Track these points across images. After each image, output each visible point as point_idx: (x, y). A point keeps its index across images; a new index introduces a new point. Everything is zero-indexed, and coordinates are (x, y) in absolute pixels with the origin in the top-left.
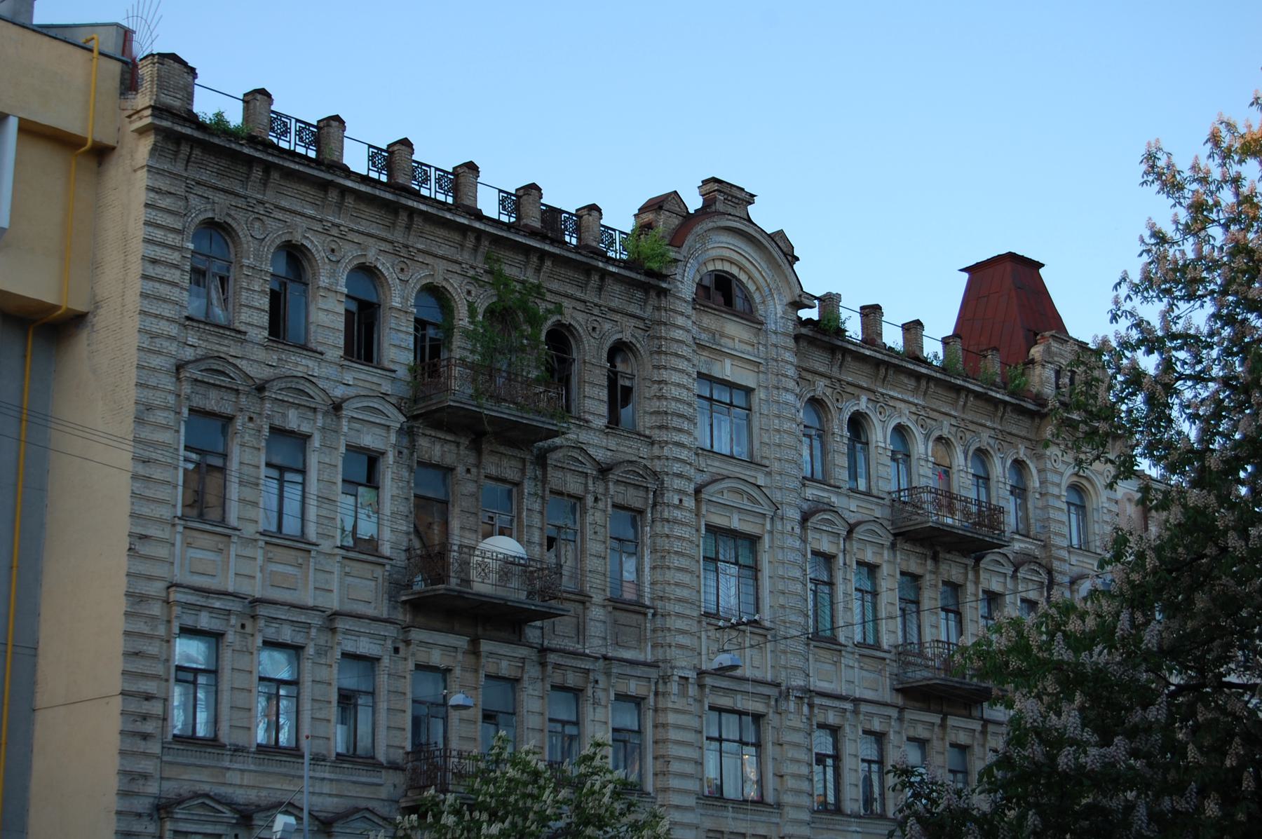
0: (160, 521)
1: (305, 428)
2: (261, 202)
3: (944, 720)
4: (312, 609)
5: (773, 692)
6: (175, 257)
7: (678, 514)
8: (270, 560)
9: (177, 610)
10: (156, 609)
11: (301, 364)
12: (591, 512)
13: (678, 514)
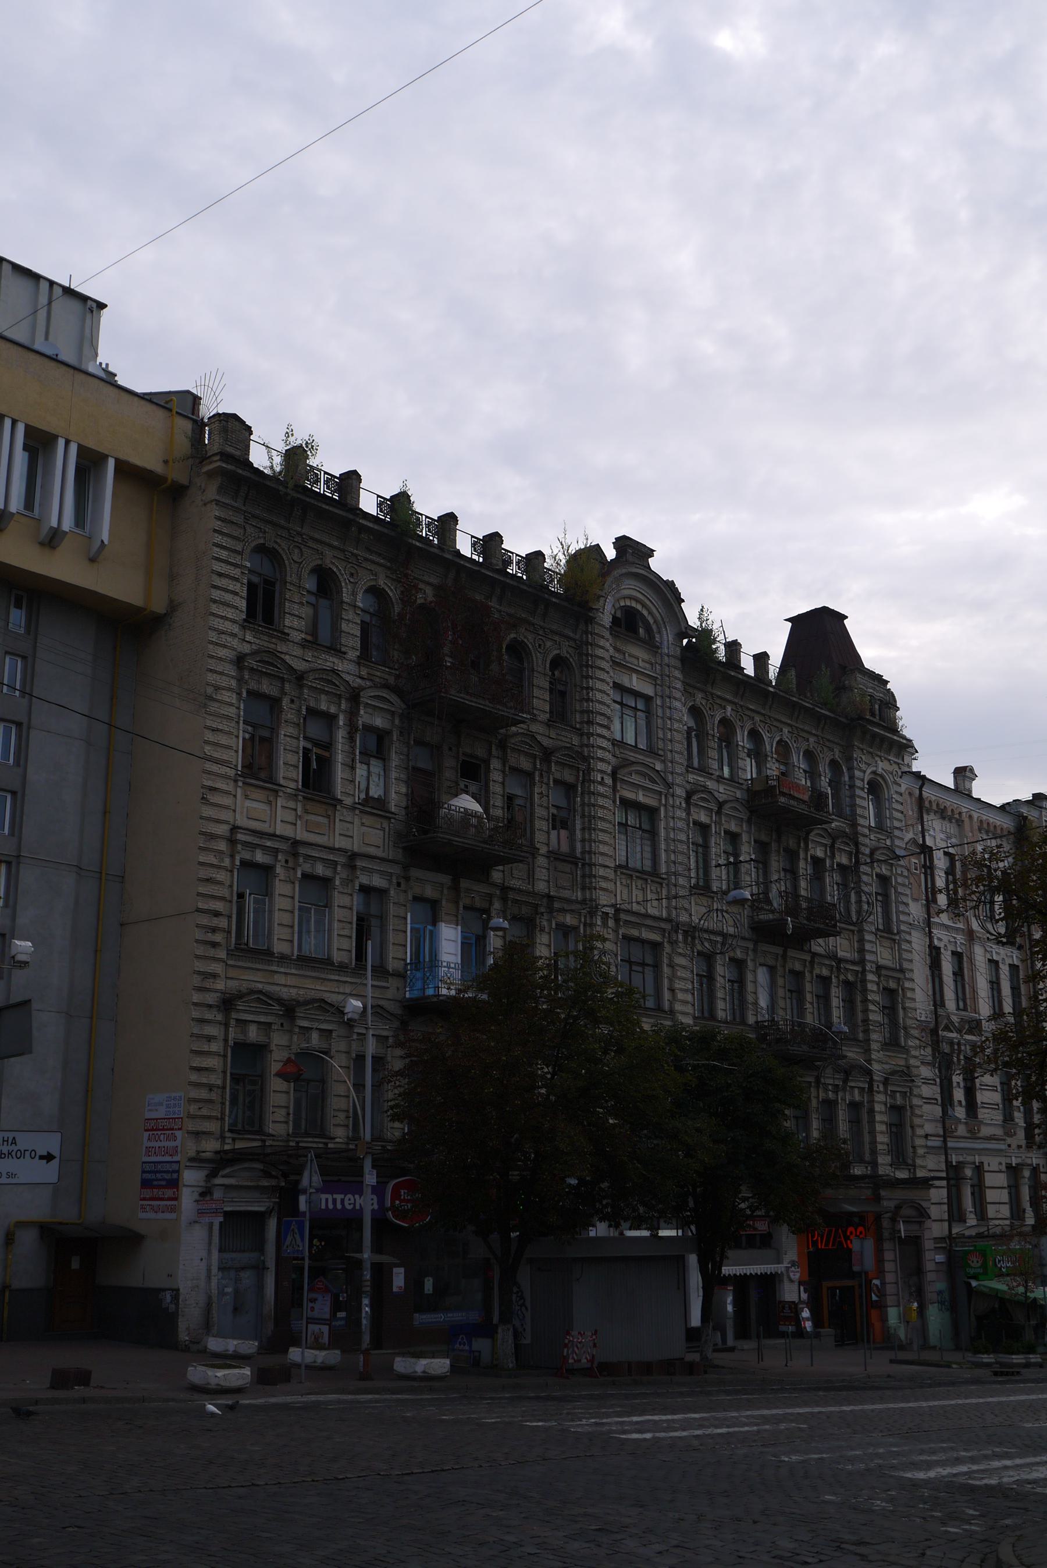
0: (225, 777)
1: (333, 710)
2: (300, 534)
3: (785, 952)
4: (339, 850)
5: (667, 926)
6: (236, 572)
7: (601, 789)
8: (306, 812)
9: (239, 847)
10: (222, 846)
11: (331, 661)
12: (538, 784)
13: (601, 789)
